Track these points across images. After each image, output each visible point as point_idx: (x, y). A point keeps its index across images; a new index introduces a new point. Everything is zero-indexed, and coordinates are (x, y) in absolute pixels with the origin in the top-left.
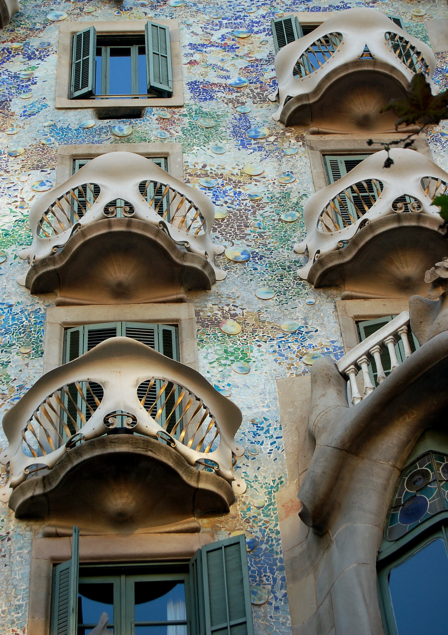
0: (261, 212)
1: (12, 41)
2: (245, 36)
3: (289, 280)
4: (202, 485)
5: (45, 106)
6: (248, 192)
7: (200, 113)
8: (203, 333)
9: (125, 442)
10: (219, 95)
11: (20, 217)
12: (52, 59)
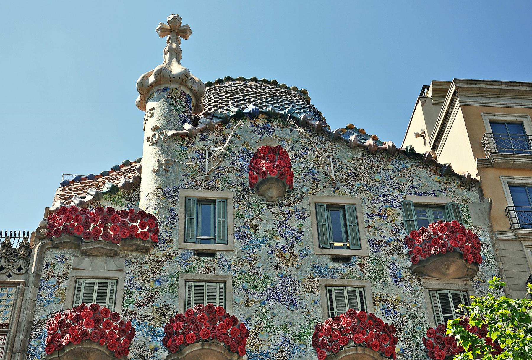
0: (406, 324)
1: (289, 205)
2: (390, 209)
5: (310, 252)
7: (375, 259)
10: (382, 248)
12: (308, 219)
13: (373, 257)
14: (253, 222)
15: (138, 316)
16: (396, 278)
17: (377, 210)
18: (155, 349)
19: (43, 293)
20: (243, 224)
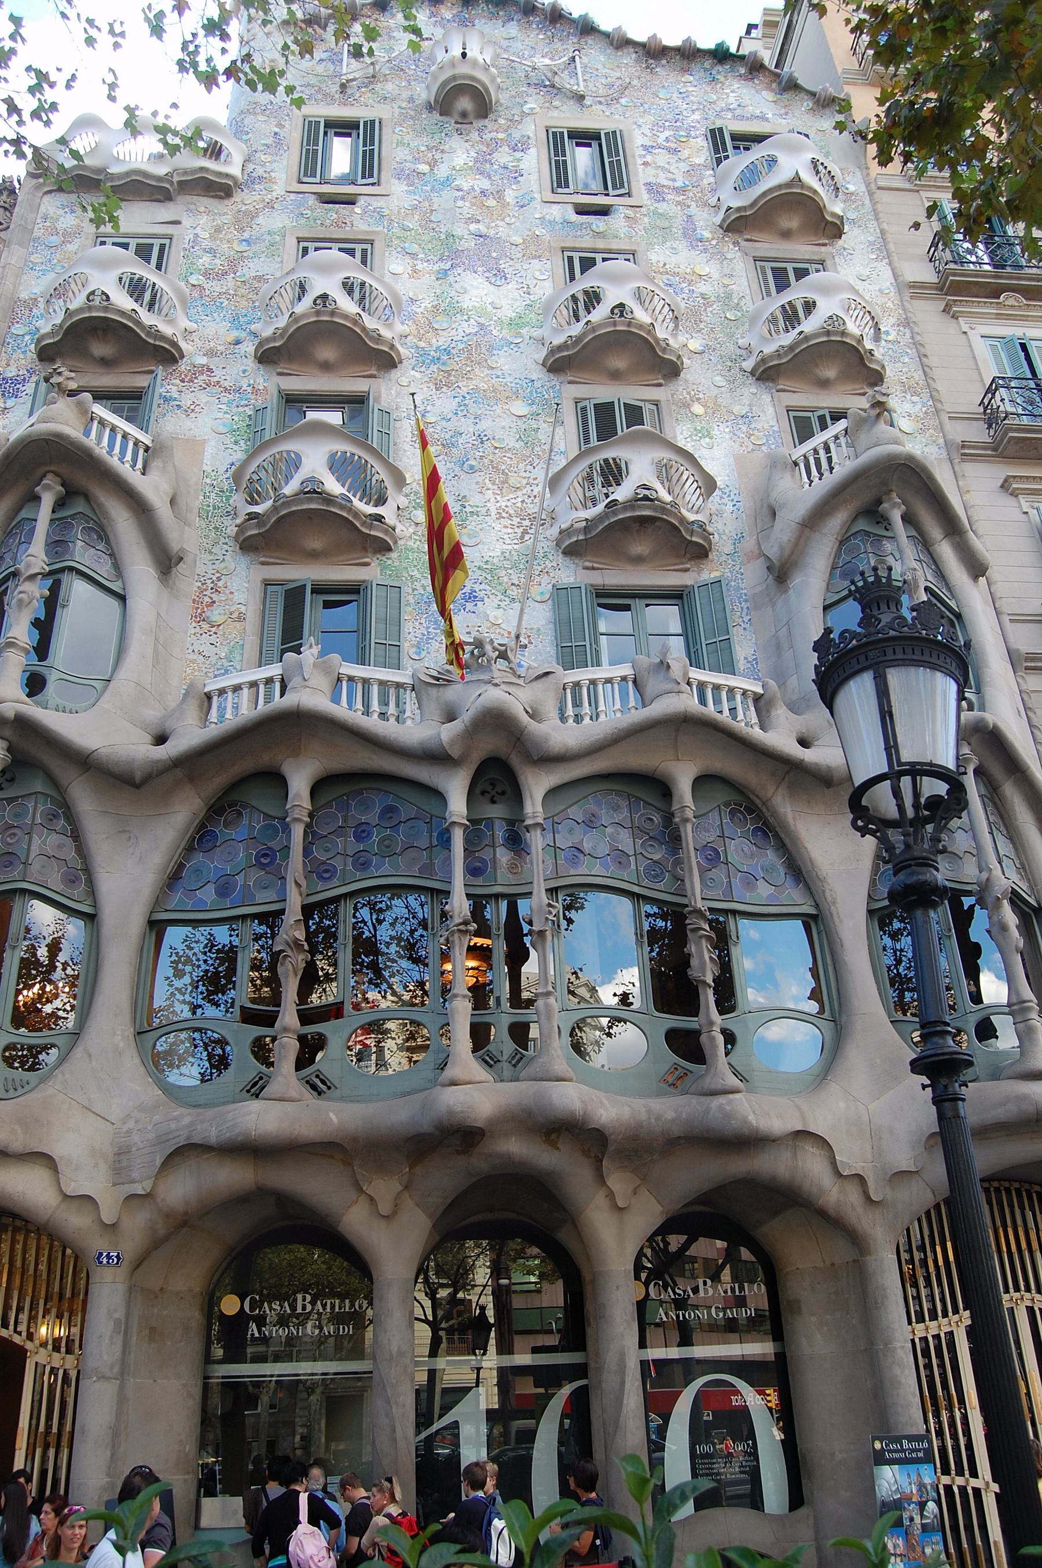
3: (735, 371)
4: (694, 539)
6: (700, 290)
7: (655, 213)
8: (678, 413)
9: (649, 508)
11: (528, 302)
12: (533, 151)
13: (652, 208)
14: (430, 155)
15: (207, 292)
16: (695, 241)
17: (660, 140)
18: (238, 342)
19: (35, 258)
20: (409, 158)
